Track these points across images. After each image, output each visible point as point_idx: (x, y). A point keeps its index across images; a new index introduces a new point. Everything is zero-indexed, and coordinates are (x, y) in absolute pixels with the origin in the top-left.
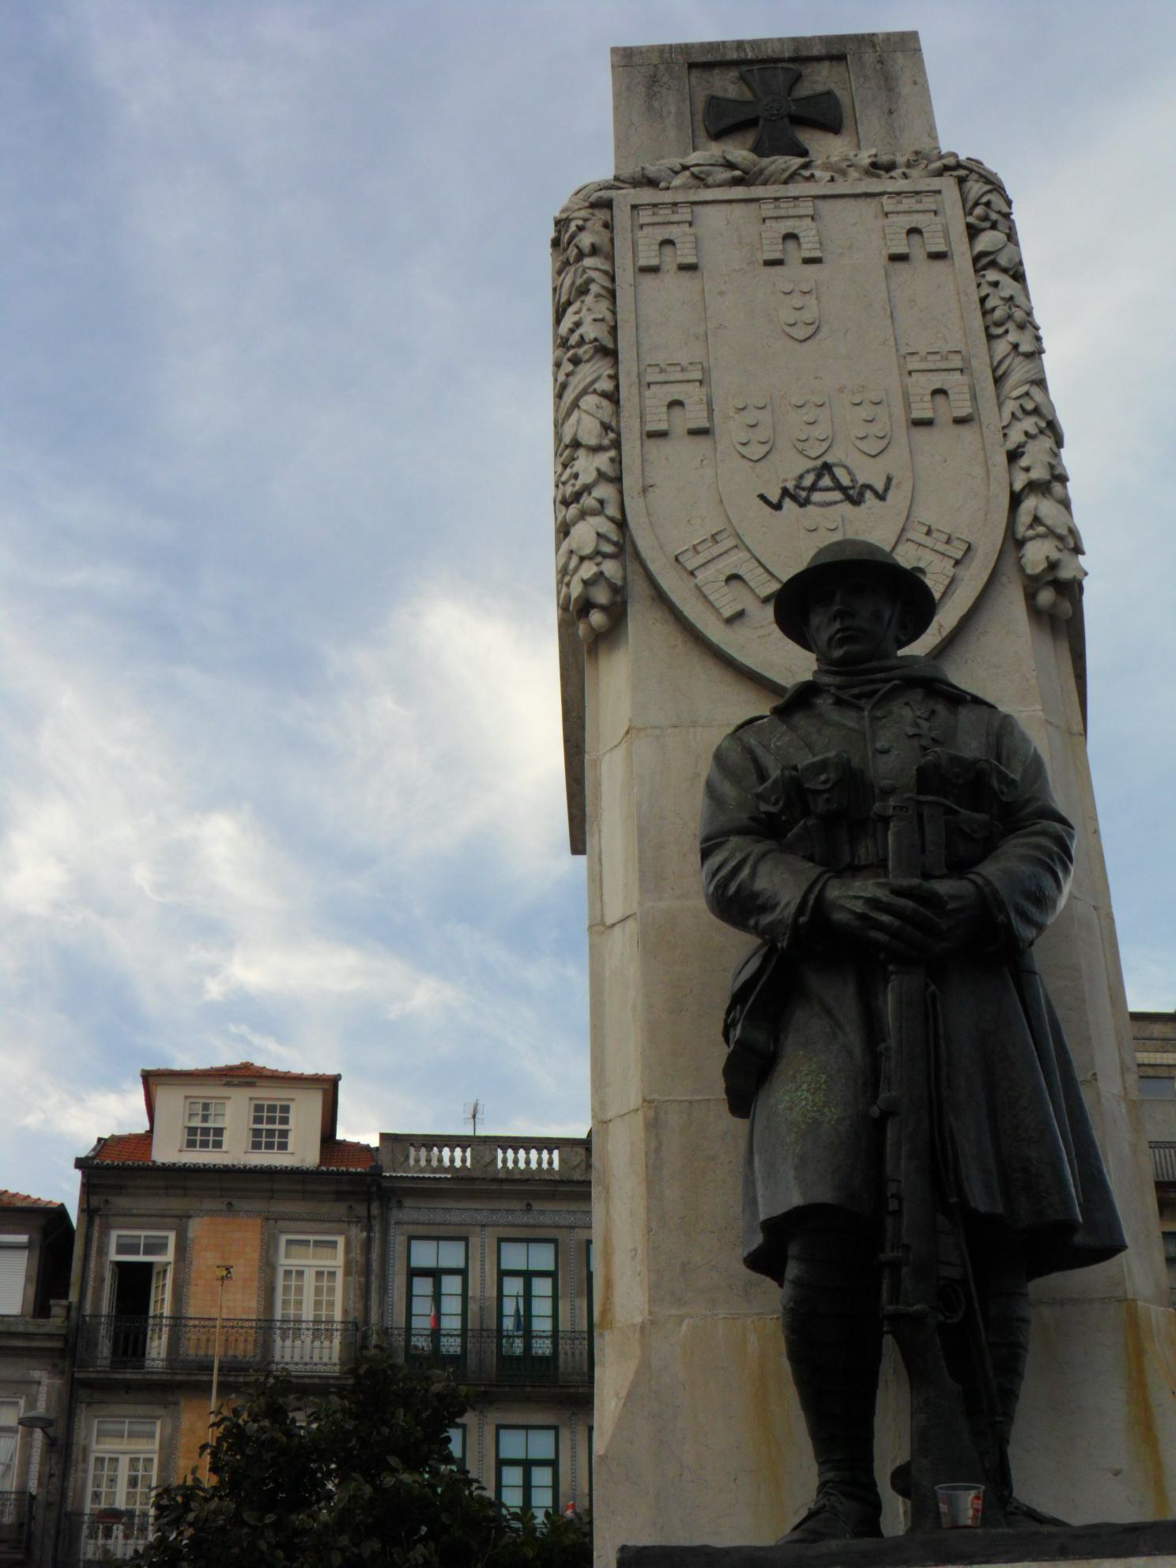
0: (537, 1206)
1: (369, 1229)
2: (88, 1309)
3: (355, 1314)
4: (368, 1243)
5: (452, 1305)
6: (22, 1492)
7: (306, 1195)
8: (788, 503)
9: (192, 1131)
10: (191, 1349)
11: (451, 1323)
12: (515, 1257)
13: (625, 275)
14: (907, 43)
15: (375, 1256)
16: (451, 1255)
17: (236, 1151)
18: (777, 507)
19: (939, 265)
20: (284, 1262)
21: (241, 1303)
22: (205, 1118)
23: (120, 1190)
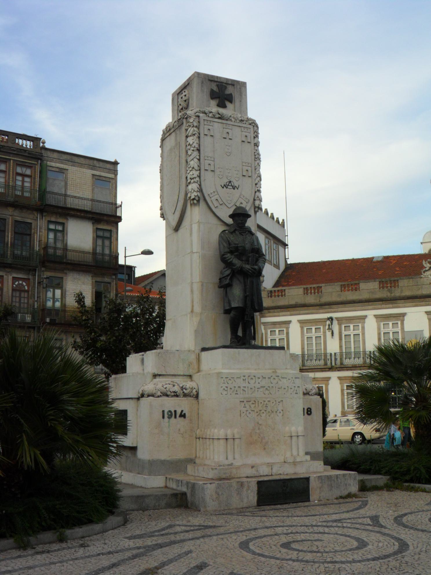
8: (225, 187)
13: (202, 135)
14: (244, 84)
18: (223, 188)
19: (249, 144)
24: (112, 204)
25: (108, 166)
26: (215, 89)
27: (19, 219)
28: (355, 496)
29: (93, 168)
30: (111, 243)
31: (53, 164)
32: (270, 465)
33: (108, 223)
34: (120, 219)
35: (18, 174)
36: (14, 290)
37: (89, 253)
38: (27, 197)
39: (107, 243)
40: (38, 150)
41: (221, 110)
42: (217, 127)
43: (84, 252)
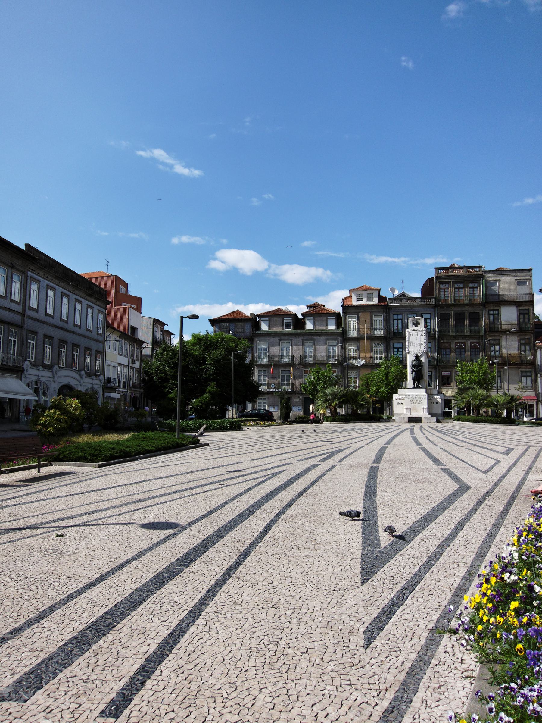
4: (387, 316)
5: (400, 324)
10: (361, 333)
11: (400, 327)
16: (400, 317)
20: (374, 319)
27: (472, 311)
30: (529, 316)
31: (490, 279)
35: (470, 288)
36: (471, 348)
39: (526, 316)
40: (481, 273)
41: (415, 328)
42: (414, 333)
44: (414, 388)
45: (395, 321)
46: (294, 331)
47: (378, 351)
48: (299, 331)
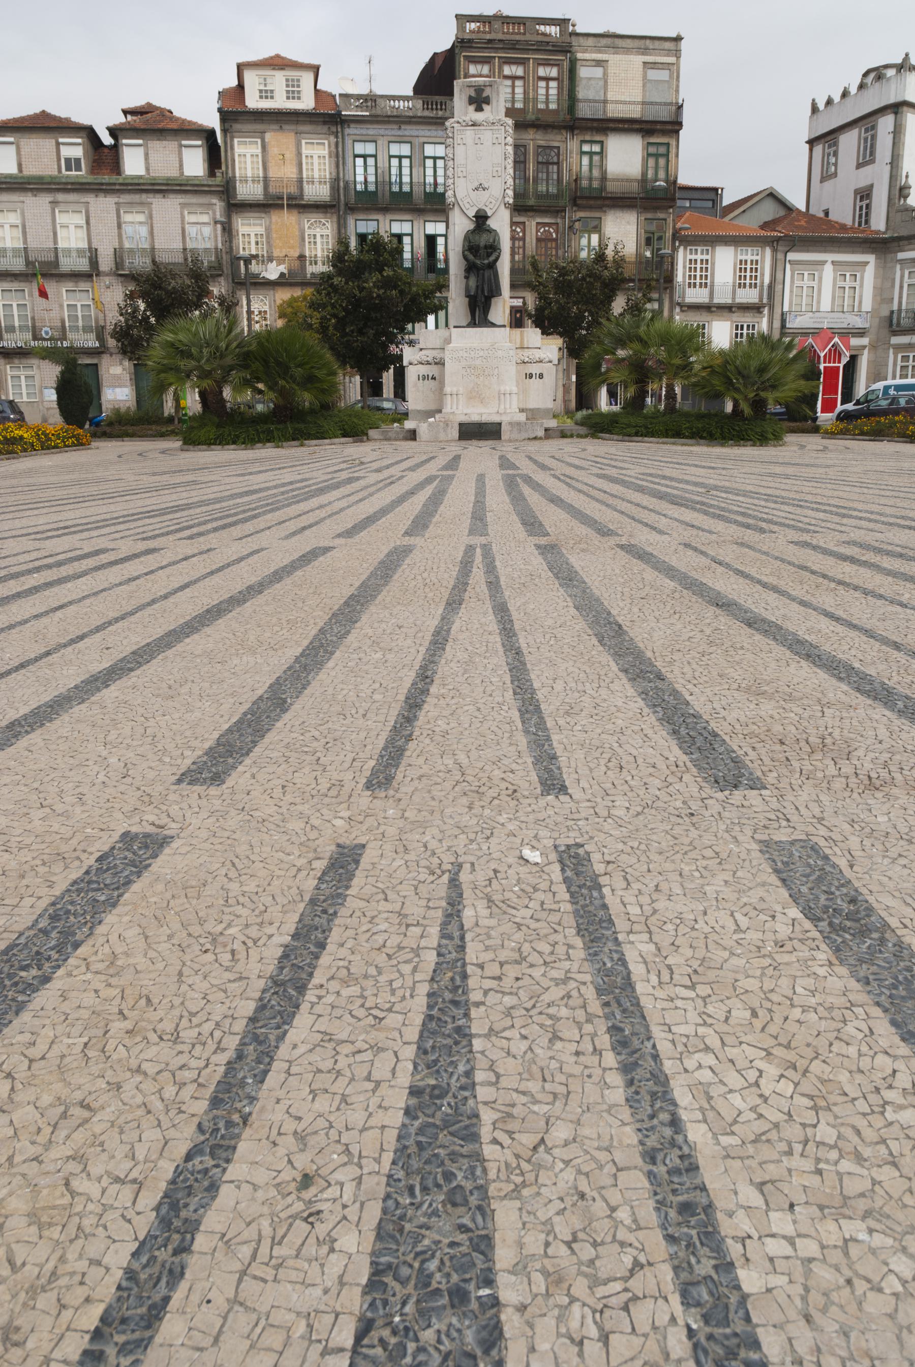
0: (403, 127)
1: (337, 137)
2: (230, 174)
3: (334, 174)
6: (216, 249)
7: (311, 123)
9: (261, 91)
10: (272, 190)
12: (395, 149)
15: (340, 149)
16: (370, 149)
17: (280, 102)
21: (290, 172)
22: (265, 85)
23: (236, 121)
24: (671, 104)
25: (667, 45)
26: (473, 94)
28: (541, 438)
29: (645, 51)
30: (668, 161)
31: (587, 56)
32: (481, 414)
33: (664, 133)
34: (680, 124)
36: (538, 240)
37: (636, 180)
38: (553, 111)
39: (662, 162)
41: (479, 117)
42: (469, 133)
43: (629, 180)
44: (473, 324)
45: (360, 161)
46: (90, 179)
47: (318, 239)
48: (106, 178)
